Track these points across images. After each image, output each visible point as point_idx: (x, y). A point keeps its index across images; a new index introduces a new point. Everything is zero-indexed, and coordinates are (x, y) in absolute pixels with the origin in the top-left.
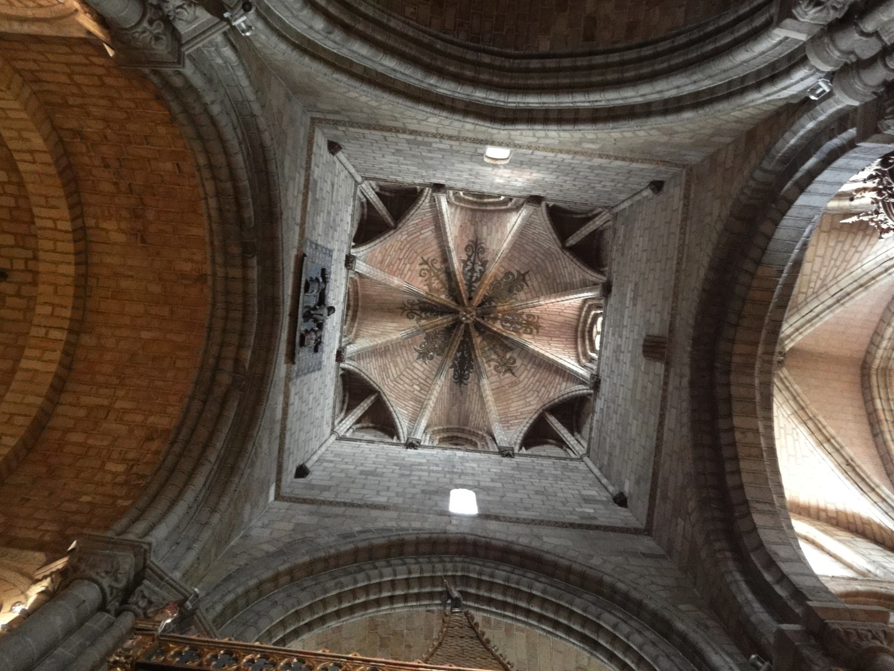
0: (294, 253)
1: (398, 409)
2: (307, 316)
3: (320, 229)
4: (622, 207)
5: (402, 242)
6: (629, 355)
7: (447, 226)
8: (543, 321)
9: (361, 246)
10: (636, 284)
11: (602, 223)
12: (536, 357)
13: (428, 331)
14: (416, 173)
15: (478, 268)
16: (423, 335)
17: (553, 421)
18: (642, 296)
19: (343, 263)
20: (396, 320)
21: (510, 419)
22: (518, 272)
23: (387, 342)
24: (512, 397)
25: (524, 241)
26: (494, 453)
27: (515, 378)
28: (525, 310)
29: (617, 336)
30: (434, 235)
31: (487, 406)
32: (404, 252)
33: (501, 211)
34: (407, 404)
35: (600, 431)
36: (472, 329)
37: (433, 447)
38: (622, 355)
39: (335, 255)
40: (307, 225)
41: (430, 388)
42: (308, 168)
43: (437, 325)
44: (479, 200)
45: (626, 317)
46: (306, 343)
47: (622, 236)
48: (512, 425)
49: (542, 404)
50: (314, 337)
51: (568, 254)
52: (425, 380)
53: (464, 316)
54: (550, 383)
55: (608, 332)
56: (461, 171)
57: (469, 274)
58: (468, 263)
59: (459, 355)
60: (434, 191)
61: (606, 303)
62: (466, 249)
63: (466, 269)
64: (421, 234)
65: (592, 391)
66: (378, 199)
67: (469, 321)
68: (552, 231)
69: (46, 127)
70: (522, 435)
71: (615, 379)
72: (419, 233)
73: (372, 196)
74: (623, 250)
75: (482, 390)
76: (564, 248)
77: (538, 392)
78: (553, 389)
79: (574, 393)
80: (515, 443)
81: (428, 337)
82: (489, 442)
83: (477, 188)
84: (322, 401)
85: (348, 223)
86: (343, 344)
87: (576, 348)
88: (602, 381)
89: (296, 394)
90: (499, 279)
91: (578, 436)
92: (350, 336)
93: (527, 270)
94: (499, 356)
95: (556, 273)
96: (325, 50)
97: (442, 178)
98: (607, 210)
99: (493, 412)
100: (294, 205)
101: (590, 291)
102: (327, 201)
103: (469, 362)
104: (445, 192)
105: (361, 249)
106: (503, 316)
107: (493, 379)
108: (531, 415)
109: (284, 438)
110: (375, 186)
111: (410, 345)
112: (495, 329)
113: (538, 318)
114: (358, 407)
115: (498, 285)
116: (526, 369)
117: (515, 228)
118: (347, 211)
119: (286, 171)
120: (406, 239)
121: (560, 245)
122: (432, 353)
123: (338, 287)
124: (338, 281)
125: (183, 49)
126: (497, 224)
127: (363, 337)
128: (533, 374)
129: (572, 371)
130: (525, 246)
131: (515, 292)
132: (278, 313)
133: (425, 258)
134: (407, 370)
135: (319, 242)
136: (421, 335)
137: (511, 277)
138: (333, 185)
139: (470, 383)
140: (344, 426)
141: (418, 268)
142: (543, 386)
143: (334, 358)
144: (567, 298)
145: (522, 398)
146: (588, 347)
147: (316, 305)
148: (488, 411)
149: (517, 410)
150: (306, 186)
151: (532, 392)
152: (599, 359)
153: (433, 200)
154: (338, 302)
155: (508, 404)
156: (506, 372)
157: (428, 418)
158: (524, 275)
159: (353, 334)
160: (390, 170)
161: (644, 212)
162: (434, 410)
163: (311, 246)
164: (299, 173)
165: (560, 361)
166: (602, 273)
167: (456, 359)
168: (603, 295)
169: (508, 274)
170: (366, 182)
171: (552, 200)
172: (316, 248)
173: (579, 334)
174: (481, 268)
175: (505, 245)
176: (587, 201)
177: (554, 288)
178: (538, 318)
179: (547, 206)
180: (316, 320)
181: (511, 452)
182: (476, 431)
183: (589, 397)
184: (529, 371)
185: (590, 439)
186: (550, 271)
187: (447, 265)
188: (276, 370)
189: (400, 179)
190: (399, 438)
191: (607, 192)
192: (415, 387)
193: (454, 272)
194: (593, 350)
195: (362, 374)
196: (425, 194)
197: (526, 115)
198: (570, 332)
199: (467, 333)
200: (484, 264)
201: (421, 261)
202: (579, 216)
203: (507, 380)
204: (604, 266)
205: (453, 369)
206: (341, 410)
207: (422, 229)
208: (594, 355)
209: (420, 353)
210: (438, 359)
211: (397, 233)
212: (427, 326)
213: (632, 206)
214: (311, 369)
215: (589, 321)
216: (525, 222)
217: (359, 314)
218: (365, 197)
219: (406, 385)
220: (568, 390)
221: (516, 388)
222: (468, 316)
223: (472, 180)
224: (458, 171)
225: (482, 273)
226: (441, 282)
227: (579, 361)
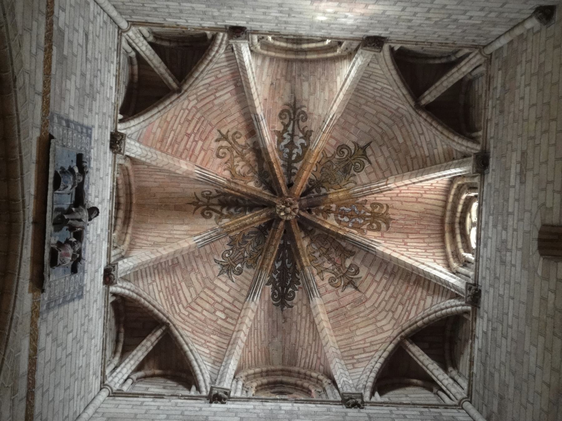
0: (36, 134)
1: (195, 347)
2: (59, 223)
3: (71, 98)
4: (497, 45)
6: (519, 253)
7: (252, 85)
8: (395, 211)
9: (132, 119)
10: (524, 154)
11: (471, 69)
12: (387, 263)
13: (232, 234)
14: (204, 13)
15: (299, 141)
17: (415, 351)
18: (532, 169)
19: (108, 144)
20: (186, 221)
21: (354, 352)
22: (356, 144)
23: (175, 252)
24: (359, 320)
25: (362, 101)
26: (335, 403)
27: (360, 294)
28: (367, 198)
29: (500, 228)
30: (234, 98)
31: (321, 336)
32: (194, 122)
33: (327, 59)
34: (208, 339)
35: (484, 364)
36: (295, 228)
37: (248, 399)
38: (508, 254)
39: (95, 134)
40: (52, 94)
41: (240, 314)
42: (50, 14)
43: (246, 225)
44: (295, 47)
45: (511, 201)
46: (59, 262)
47: (499, 86)
48: (358, 361)
49: (399, 329)
50: (71, 251)
51: (424, 115)
52: (232, 304)
53: (283, 210)
54: (409, 299)
55: (487, 223)
56: (268, 8)
57: (287, 150)
58: (285, 135)
59: (278, 265)
60: (230, 37)
61: (482, 181)
62: (281, 115)
63: (283, 144)
64: (215, 99)
65: (469, 308)
66: (153, 52)
67: (289, 218)
68: (400, 84)
70: (373, 375)
71: (501, 289)
73: (144, 48)
74: (502, 105)
75: (314, 314)
76: (418, 107)
77: (393, 312)
78: (415, 308)
79: (444, 311)
80: (365, 387)
81: (232, 243)
82: (327, 387)
83: (291, 30)
84: (86, 340)
85: (111, 88)
86: (113, 259)
87: (444, 247)
88: (483, 293)
89: (48, 335)
90: (329, 155)
91: (454, 373)
92: (122, 247)
93: (369, 141)
94: (335, 264)
95: (409, 143)
97: (242, 19)
98: (477, 51)
99: (331, 344)
100: (33, 67)
101: (459, 165)
102: (79, 58)
103: (294, 276)
104: (247, 38)
105: (133, 123)
106: (338, 207)
107: (329, 297)
108: (385, 345)
109: (33, 399)
110: (147, 34)
111: (208, 255)
112: (327, 226)
113: (388, 207)
114: (139, 347)
115: (329, 164)
116: (373, 280)
117: (348, 82)
118: (109, 71)
119: (19, 18)
120: (194, 107)
121: (413, 104)
122: (239, 265)
123: (101, 178)
124: (102, 171)
126: (323, 79)
127: (141, 247)
128: (385, 287)
129: (440, 279)
130: (363, 107)
131: (352, 172)
132: (17, 221)
133: (224, 131)
134: (206, 290)
135: (72, 117)
136: (223, 240)
137: (346, 152)
138: (87, 35)
139: (296, 304)
140: (120, 376)
141: (214, 145)
142: (400, 303)
144: (426, 177)
145: (371, 322)
146: (460, 245)
147: (71, 206)
148: (324, 344)
149: (364, 339)
150: (49, 38)
151: (384, 313)
152: (477, 260)
153: (230, 49)
154: (103, 200)
155: (352, 331)
156: (345, 286)
157: (238, 358)
158: (364, 149)
159: (127, 243)
160: (167, 10)
161: (529, 50)
162: (247, 346)
163: (60, 123)
164: (37, 20)
165: (422, 267)
166: (474, 140)
167: (274, 271)
168: (477, 172)
169: (341, 148)
170: (133, 28)
171: (398, 42)
172: (68, 126)
173: (447, 228)
174: (303, 141)
175: (335, 108)
176: (447, 39)
177: (406, 164)
178: (388, 207)
179: (391, 49)
180: (72, 228)
181: (359, 401)
182: (308, 373)
183: (465, 316)
184: (379, 283)
185: (471, 375)
186: (401, 140)
187: (254, 140)
188: (18, 302)
189: (182, 22)
190: (198, 389)
191: (473, 25)
192: (219, 314)
193: (265, 149)
194: (468, 248)
195: (143, 300)
196: (219, 42)
198: (435, 225)
199: (288, 234)
200: (307, 135)
201: (217, 136)
202: (437, 62)
203: (348, 297)
204: (477, 130)
205: (271, 286)
206: (115, 352)
207: (217, 90)
208: (469, 256)
209: (224, 266)
210: (249, 273)
211: (182, 98)
212: (232, 228)
213: (511, 42)
214: (68, 298)
215: (460, 208)
216: (362, 73)
217: (133, 215)
218: (134, 49)
219: (205, 313)
220: (434, 308)
221: (362, 308)
222: (289, 210)
223: (285, 19)
224: (264, 7)
225: (305, 148)
226: (248, 163)
227: (448, 266)
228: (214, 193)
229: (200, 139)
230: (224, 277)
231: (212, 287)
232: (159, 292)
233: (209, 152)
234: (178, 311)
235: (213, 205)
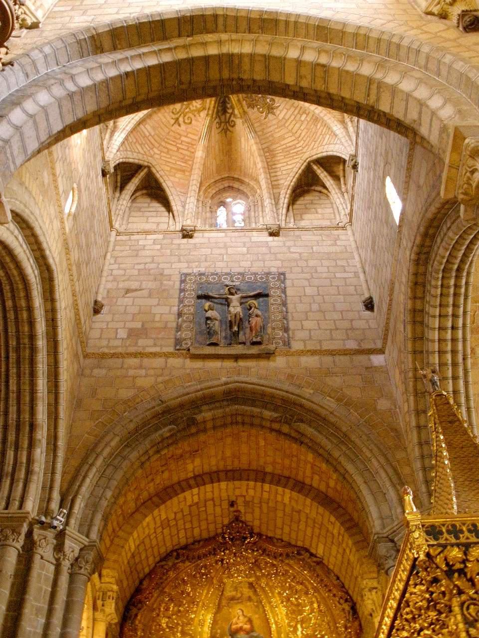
5: (161, 152)
16: (250, 111)
20: (239, 139)
34: (320, 131)
64: (150, 135)
69: (138, 516)
72: (150, 137)
96: (48, 429)
111: (261, 125)
120: (157, 148)
122: (268, 100)
125: (87, 544)
133: (173, 121)
134: (287, 125)
141: (183, 127)
143: (276, 238)
192: (303, 118)
197: (41, 261)
201: (176, 126)
207: (145, 136)
217: (236, 176)
219: (302, 128)
228: (217, 120)
229: (180, 138)
230: (277, 112)
231: (284, 121)
232: (287, 165)
233: (188, 130)
234: (301, 148)
235: (225, 119)
